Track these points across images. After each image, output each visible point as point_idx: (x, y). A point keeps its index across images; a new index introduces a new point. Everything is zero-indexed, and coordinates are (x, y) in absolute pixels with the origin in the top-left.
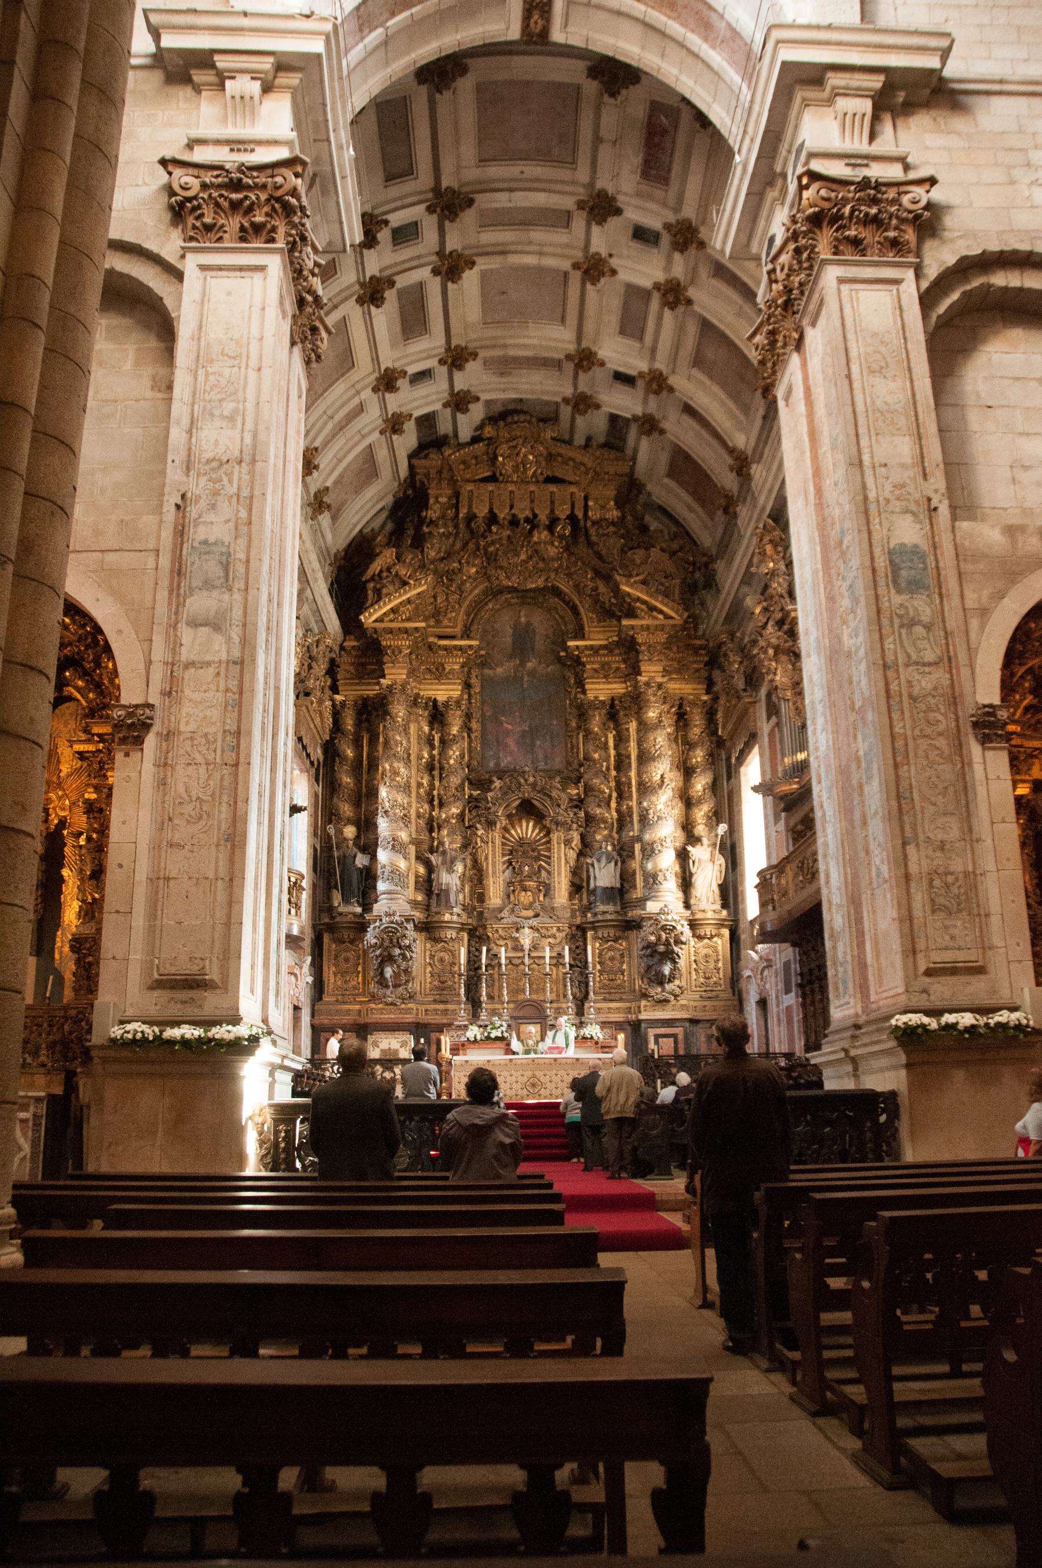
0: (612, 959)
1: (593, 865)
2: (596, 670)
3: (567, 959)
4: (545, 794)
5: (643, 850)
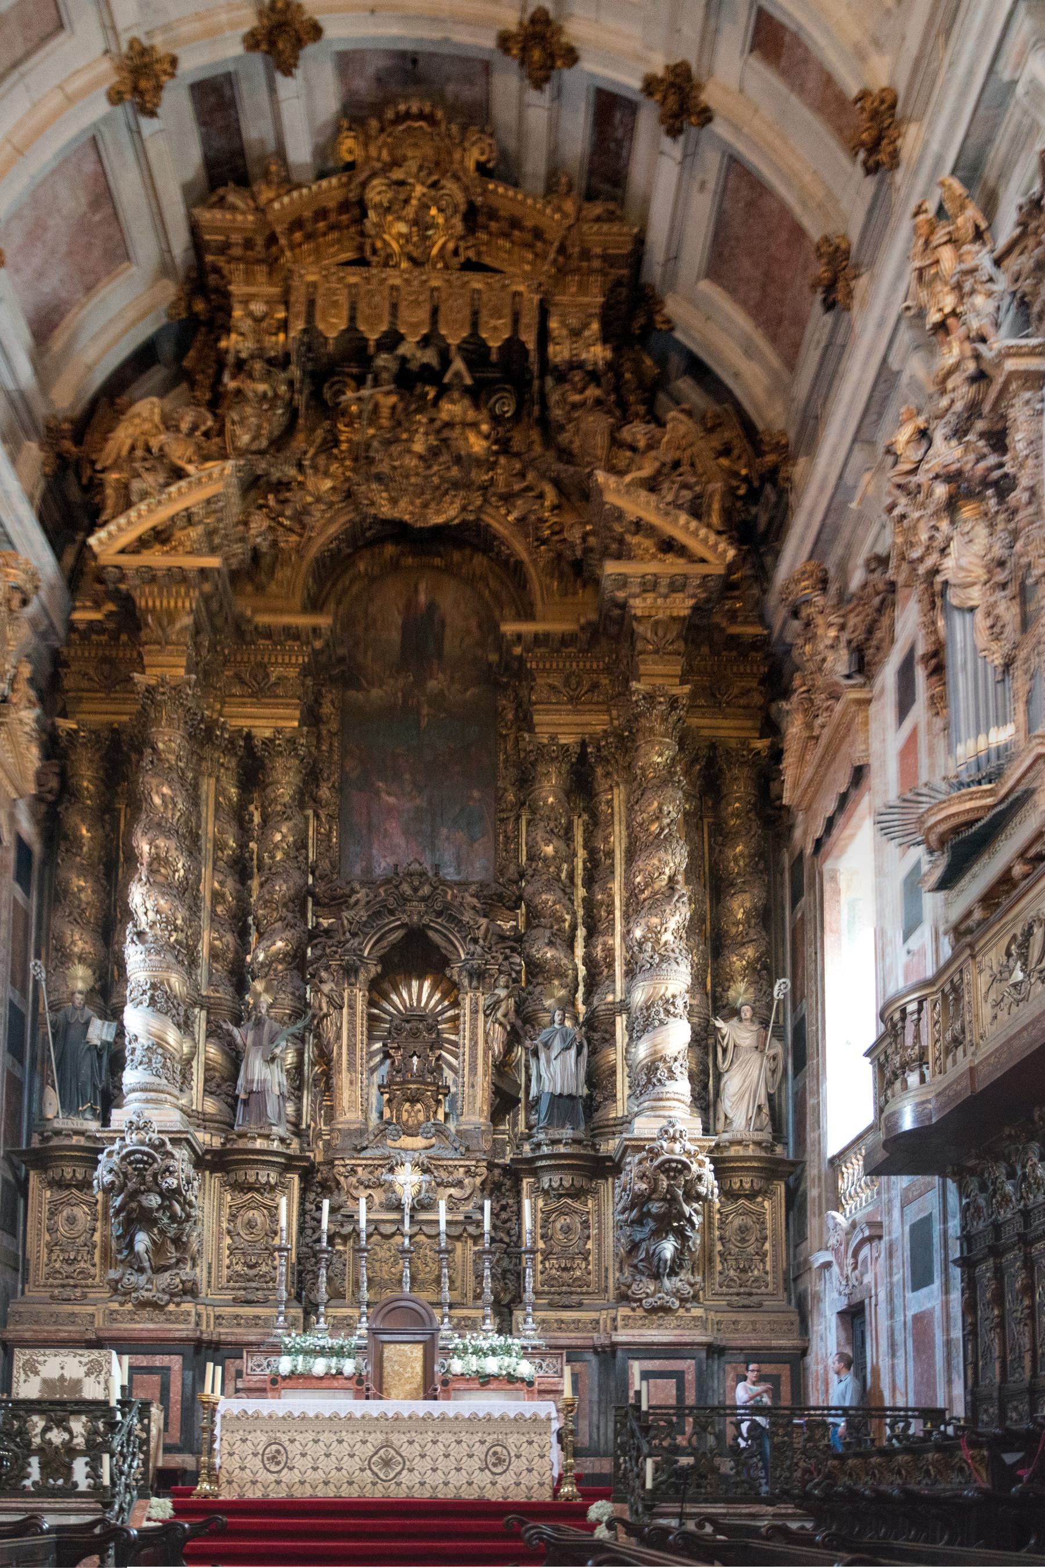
0: (567, 1230)
1: (536, 1054)
2: (553, 688)
3: (487, 1226)
4: (452, 918)
5: (630, 1028)
